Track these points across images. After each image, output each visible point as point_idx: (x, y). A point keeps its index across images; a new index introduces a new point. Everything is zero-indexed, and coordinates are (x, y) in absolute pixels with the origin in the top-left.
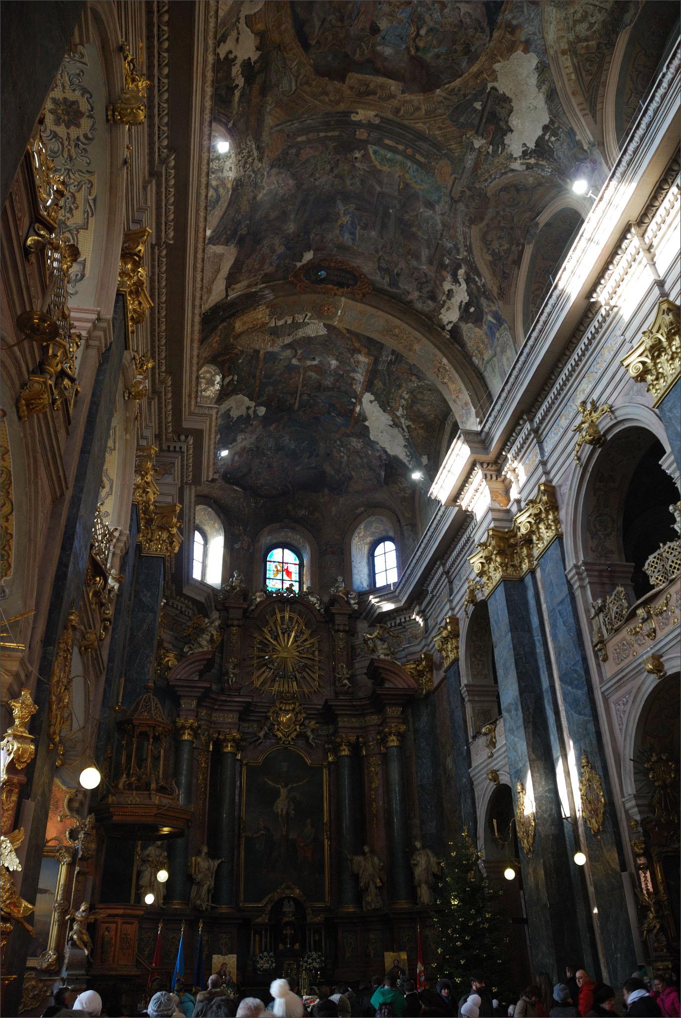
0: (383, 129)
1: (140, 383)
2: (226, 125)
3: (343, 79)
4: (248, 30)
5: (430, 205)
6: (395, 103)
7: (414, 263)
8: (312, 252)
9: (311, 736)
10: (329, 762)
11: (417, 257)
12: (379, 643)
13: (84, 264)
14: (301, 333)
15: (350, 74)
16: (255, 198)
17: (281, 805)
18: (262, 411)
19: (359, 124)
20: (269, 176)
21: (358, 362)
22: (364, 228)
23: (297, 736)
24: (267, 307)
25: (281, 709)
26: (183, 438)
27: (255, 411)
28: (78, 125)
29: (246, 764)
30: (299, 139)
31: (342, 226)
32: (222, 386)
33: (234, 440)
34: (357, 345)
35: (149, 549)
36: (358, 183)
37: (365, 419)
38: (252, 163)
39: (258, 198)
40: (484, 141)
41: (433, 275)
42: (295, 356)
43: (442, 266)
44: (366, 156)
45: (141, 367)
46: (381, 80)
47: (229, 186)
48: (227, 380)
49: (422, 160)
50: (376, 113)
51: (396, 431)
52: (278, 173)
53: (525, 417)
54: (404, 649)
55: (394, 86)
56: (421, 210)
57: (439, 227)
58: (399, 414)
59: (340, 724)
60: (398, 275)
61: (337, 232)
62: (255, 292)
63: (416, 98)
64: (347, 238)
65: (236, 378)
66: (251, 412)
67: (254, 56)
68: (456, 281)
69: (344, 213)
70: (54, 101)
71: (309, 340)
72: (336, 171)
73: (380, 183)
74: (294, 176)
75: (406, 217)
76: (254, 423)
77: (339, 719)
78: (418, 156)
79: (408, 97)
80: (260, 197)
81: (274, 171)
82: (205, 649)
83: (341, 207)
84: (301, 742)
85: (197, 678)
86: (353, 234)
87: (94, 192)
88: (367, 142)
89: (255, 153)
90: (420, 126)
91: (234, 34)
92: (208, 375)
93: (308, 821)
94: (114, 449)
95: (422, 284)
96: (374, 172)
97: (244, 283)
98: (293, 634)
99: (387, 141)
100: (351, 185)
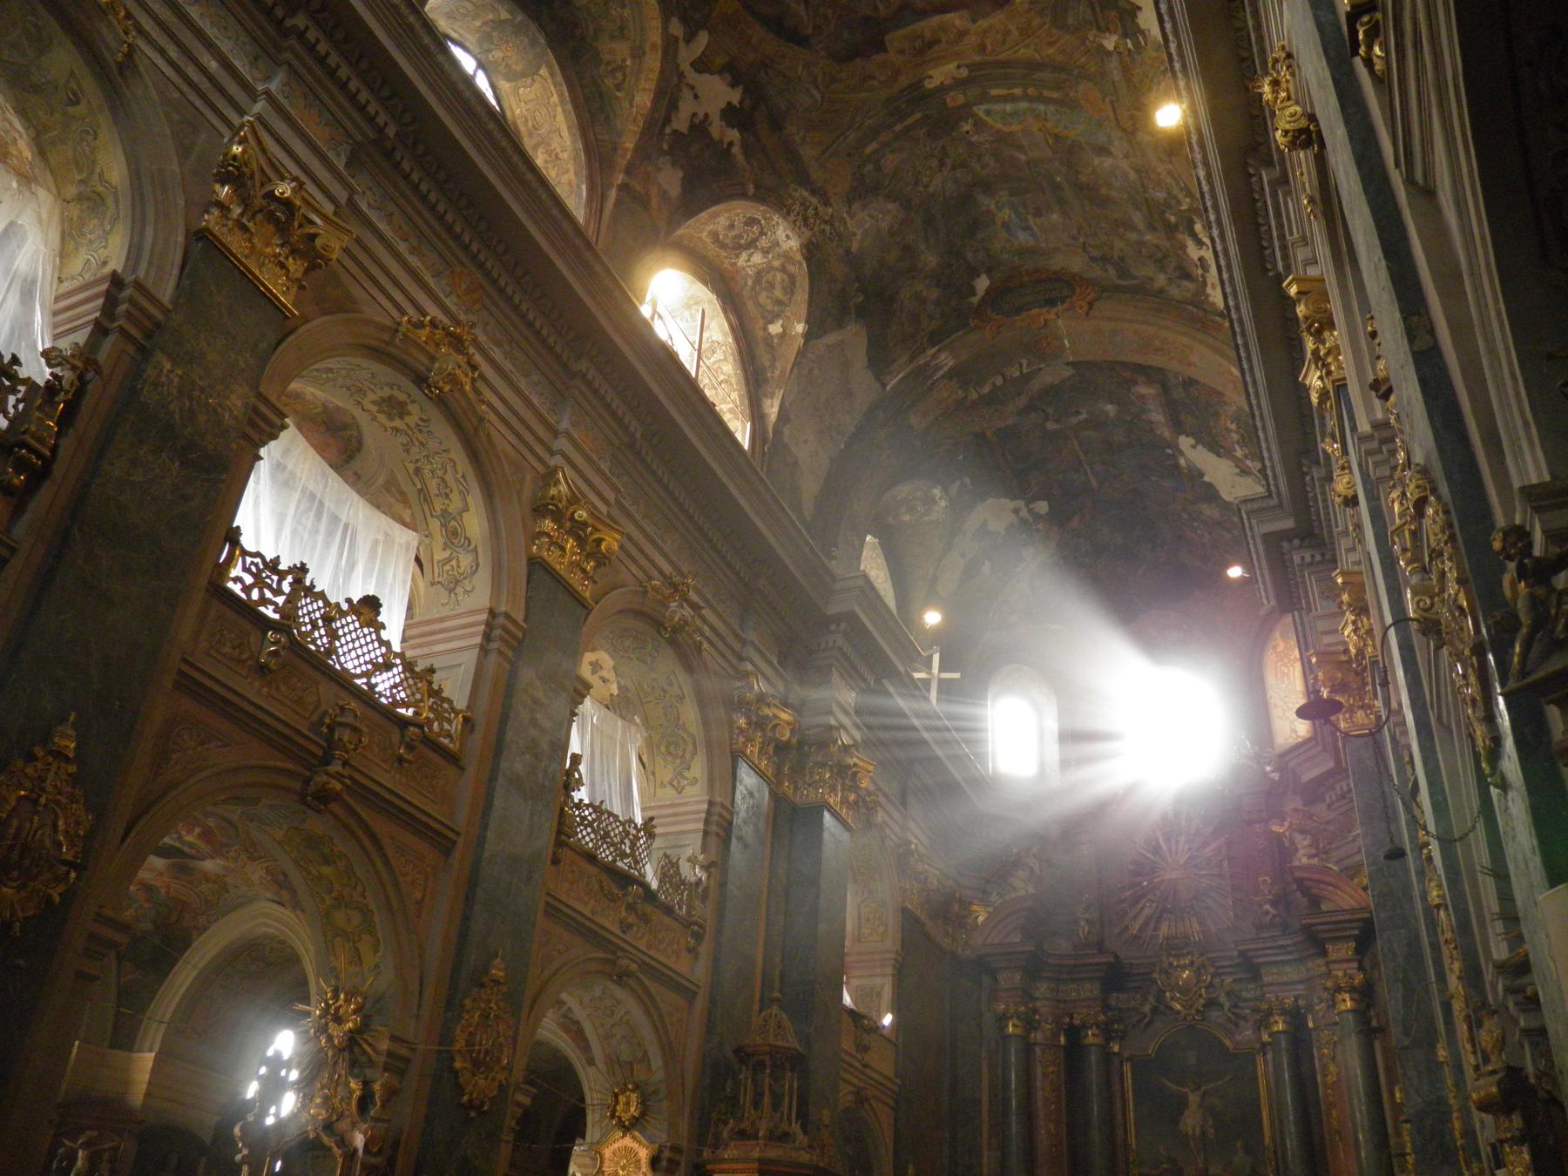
0: (981, 76)
1: (674, 612)
2: (744, 196)
3: (881, 47)
4: (706, 76)
5: (1103, 151)
6: (972, 39)
7: (1133, 236)
8: (984, 277)
9: (1227, 1005)
10: (1264, 1045)
11: (1131, 227)
12: (1298, 837)
13: (475, 550)
14: (1036, 385)
15: (887, 37)
16: (848, 252)
17: (1191, 1121)
19: (942, 89)
20: (852, 216)
21: (1143, 396)
22: (1038, 213)
24: (950, 379)
25: (1171, 964)
26: (833, 627)
28: (409, 413)
29: (1130, 1059)
30: (869, 150)
31: (1005, 225)
34: (1128, 374)
36: (992, 163)
37: (1201, 474)
38: (817, 214)
39: (854, 248)
40: (1115, 38)
41: (1166, 244)
42: (1047, 418)
43: (1171, 229)
44: (979, 125)
45: (676, 590)
46: (935, 20)
47: (799, 257)
49: (1055, 95)
50: (955, 64)
52: (864, 207)
55: (956, 19)
56: (1096, 162)
57: (1133, 175)
58: (1239, 453)
59: (1267, 979)
60: (1122, 259)
61: (1004, 235)
62: (927, 364)
63: (997, 19)
64: (1023, 238)
67: (735, 96)
68: (1200, 243)
69: (1000, 208)
70: (373, 402)
71: (1052, 392)
72: (949, 162)
73: (1020, 148)
74: (890, 197)
75: (1083, 179)
77: (1263, 971)
78: (1046, 93)
79: (983, 23)
80: (855, 248)
81: (856, 206)
82: (1022, 893)
83: (986, 202)
84: (1214, 1014)
85: (1018, 939)
86: (1027, 228)
87: (459, 469)
88: (968, 106)
89: (814, 201)
90: (1023, 53)
91: (687, 94)
93: (1239, 1144)
95: (1160, 261)
96: (1002, 138)
97: (905, 359)
99: (994, 92)
100: (983, 168)
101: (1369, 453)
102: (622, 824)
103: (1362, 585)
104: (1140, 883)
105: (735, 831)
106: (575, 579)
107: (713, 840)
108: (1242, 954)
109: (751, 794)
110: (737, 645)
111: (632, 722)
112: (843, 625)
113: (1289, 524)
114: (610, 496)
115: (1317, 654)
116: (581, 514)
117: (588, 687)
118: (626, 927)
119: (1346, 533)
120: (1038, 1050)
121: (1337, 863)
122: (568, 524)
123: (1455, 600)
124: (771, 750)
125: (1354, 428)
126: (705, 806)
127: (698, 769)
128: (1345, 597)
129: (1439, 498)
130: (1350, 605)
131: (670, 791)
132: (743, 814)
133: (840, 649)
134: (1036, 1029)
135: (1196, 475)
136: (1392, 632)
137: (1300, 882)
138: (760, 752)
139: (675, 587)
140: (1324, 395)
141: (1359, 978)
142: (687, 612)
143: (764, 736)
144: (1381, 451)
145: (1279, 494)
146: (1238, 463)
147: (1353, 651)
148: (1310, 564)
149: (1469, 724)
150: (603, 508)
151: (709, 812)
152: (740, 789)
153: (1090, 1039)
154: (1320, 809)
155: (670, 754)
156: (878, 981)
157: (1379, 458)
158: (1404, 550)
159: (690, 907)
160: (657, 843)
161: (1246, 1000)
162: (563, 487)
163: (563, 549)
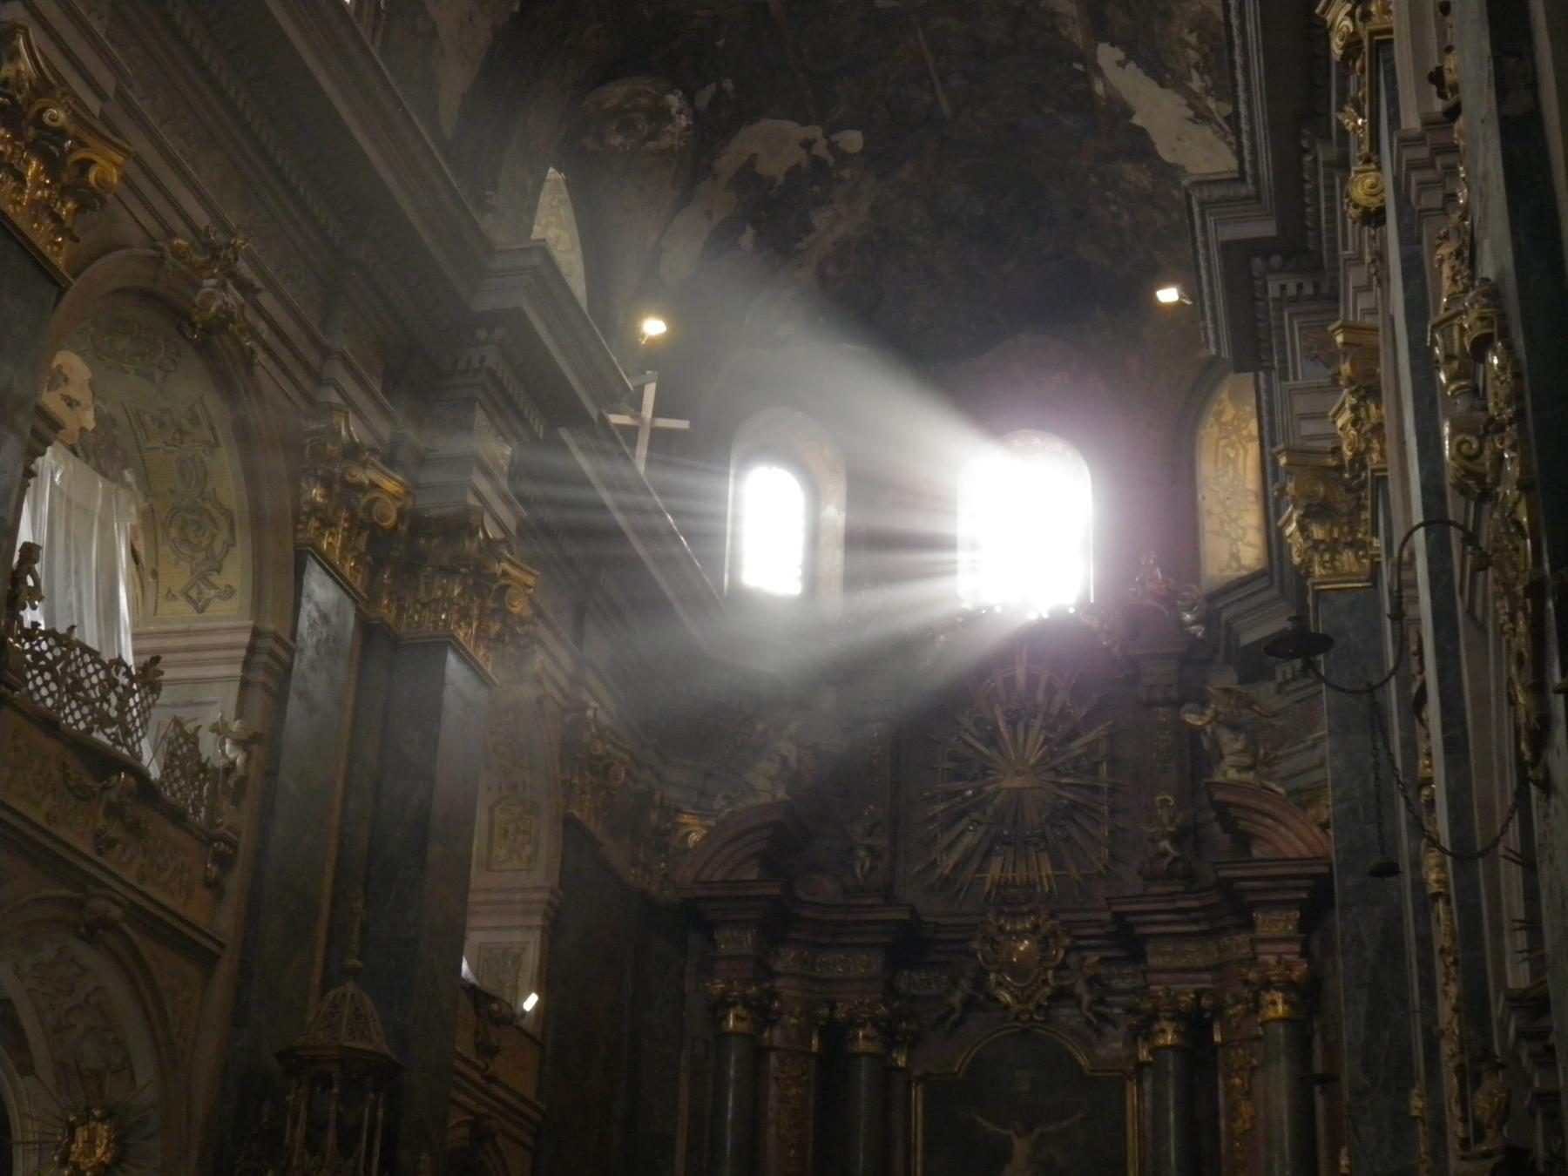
9: (1086, 999)
10: (1141, 1065)
12: (1225, 736)
18: (853, 140)
23: (1049, 999)
25: (1001, 929)
26: (481, 334)
27: (832, 147)
32: (696, 116)
33: (809, 228)
35: (419, 624)
37: (1128, 112)
45: (215, 257)
48: (704, 97)
51: (1207, 131)
53: (1306, 132)
54: (1314, 746)
58: (1196, 84)
59: (1154, 961)
65: (728, 85)
66: (820, 149)
76: (846, 173)
77: (1149, 948)
82: (765, 798)
84: (1064, 1013)
85: (754, 877)
92: (644, 101)
94: (217, 445)
98: (1037, 723)
101: (1414, 166)
102: (106, 667)
103: (1376, 349)
104: (961, 792)
105: (295, 682)
106: (39, 232)
107: (257, 699)
108: (1119, 917)
109: (325, 618)
110: (313, 358)
111: (118, 479)
112: (499, 332)
113: (1265, 228)
114: (108, 83)
115: (1289, 451)
116: (57, 115)
117: (56, 425)
118: (103, 843)
119: (1359, 259)
120: (773, 1058)
121: (1283, 781)
122: (31, 133)
123: (1513, 512)
124: (362, 542)
125: (1394, 119)
126: (245, 638)
127: (236, 572)
128: (1346, 368)
129: (1509, 347)
130: (1351, 382)
131: (182, 605)
132: (310, 653)
133: (492, 374)
134: (771, 1024)
135: (1120, 111)
136: (1420, 534)
137: (1222, 809)
138: (344, 547)
139: (213, 251)
140: (1353, 45)
141: (1300, 970)
142: (233, 297)
143: (352, 518)
144: (1432, 166)
145: (1257, 180)
146: (1192, 99)
147: (1348, 454)
148: (1295, 300)
149: (1510, 682)
150: (95, 105)
151: (252, 649)
152: (307, 609)
153: (862, 1045)
154: (1264, 693)
155: (186, 541)
156: (518, 937)
157: (1429, 175)
158: (1449, 358)
159: (213, 812)
160: (166, 696)
161: (1122, 992)
162: (25, 65)
163: (20, 177)
